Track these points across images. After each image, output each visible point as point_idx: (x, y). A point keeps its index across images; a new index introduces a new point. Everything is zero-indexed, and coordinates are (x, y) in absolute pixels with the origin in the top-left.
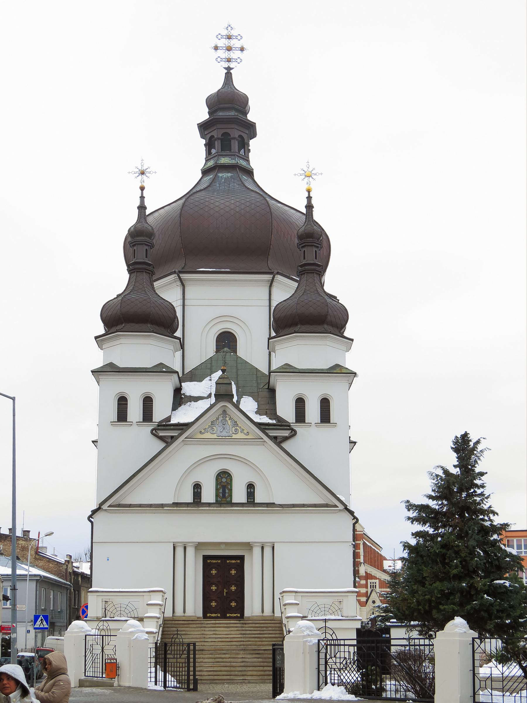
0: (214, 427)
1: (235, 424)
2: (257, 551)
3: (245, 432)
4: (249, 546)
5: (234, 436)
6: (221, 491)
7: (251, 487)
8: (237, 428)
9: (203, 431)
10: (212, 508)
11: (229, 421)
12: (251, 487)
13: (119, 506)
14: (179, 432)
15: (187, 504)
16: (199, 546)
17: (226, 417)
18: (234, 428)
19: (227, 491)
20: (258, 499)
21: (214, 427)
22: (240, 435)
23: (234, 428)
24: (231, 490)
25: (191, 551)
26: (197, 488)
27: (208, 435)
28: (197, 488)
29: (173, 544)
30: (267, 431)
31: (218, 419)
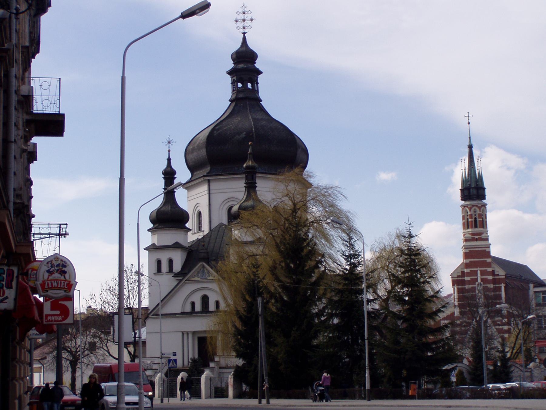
1: (209, 272)
5: (209, 278)
7: (217, 303)
11: (206, 271)
12: (217, 303)
22: (211, 278)
26: (193, 304)
27: (196, 278)
28: (193, 304)
31: (200, 270)
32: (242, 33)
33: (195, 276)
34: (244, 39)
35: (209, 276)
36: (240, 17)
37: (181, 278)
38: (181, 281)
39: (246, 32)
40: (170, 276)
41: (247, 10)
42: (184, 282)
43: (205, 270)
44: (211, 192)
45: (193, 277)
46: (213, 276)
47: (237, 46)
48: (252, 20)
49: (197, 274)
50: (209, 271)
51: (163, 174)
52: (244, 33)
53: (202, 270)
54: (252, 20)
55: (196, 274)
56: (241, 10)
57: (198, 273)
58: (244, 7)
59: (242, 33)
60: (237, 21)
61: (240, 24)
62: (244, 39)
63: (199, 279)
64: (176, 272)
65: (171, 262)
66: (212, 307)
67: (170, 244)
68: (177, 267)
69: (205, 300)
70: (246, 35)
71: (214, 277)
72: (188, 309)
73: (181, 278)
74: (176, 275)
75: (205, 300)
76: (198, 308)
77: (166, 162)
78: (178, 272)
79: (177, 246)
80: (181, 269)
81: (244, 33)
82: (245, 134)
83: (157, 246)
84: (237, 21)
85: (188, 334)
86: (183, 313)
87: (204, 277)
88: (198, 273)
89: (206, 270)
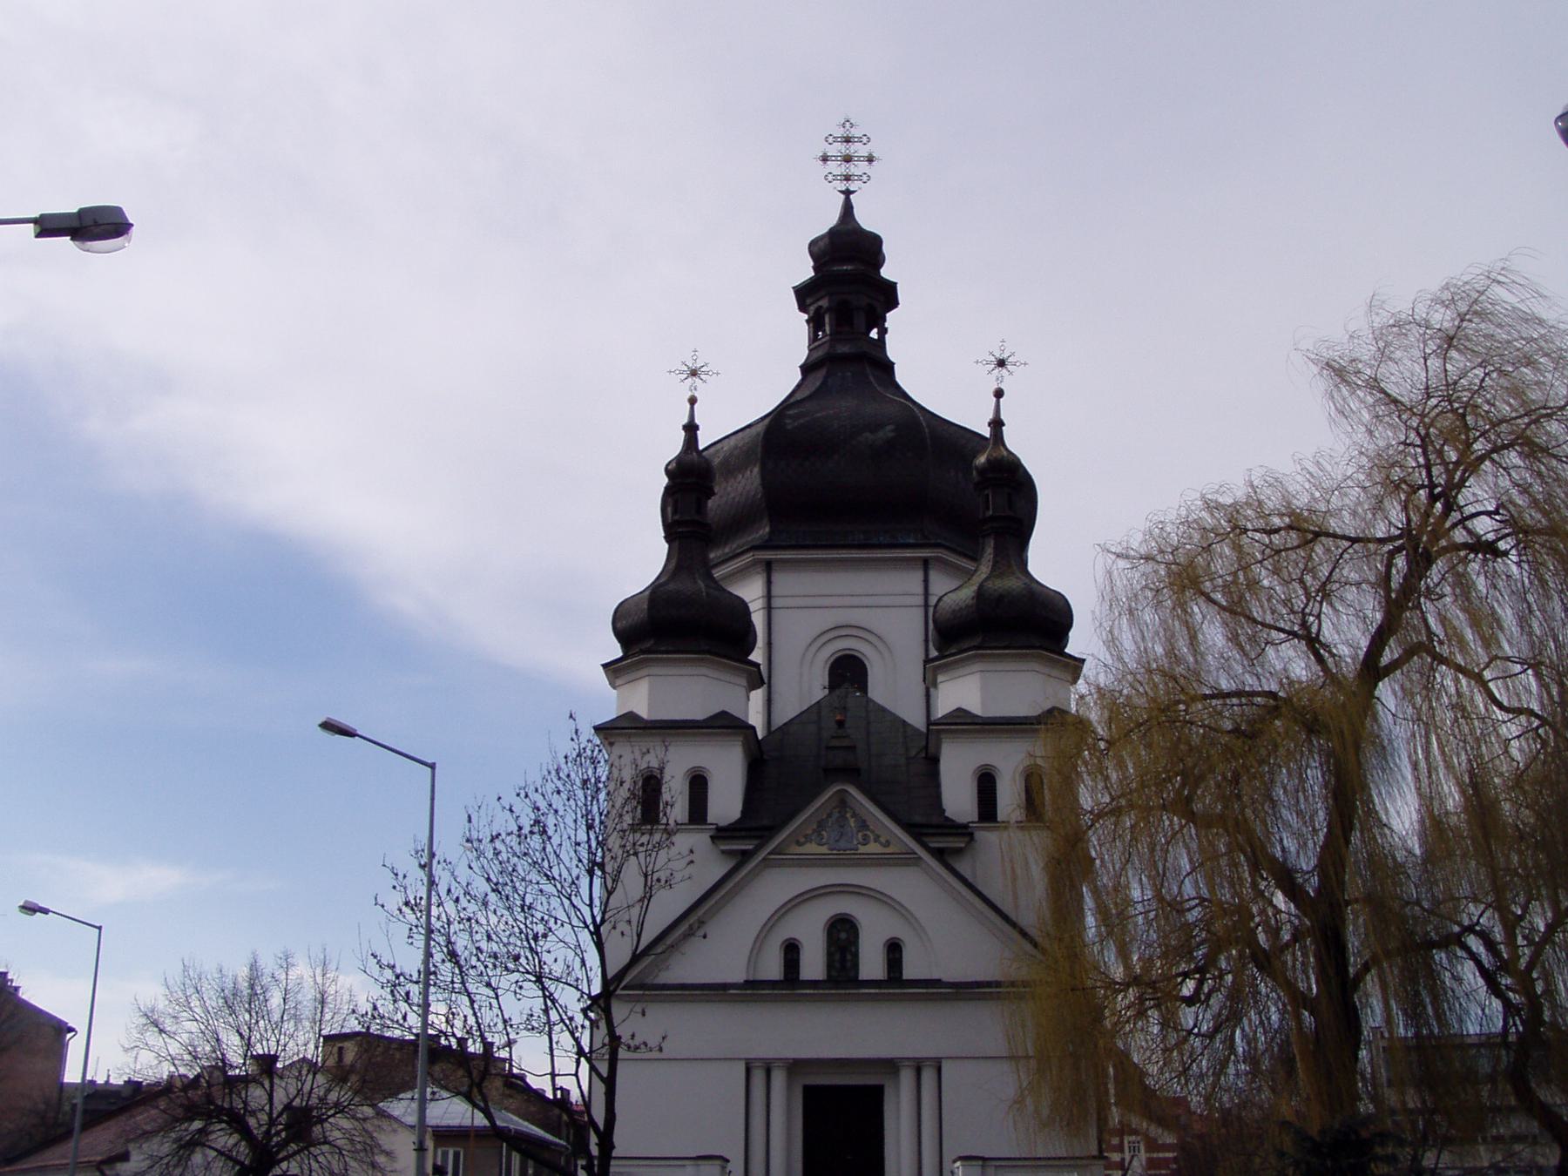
0: (824, 833)
1: (863, 825)
2: (906, 1077)
3: (883, 840)
4: (891, 1066)
5: (862, 849)
6: (837, 957)
7: (894, 949)
8: (868, 833)
9: (802, 840)
10: (821, 991)
11: (852, 822)
12: (894, 949)
13: (643, 986)
14: (756, 842)
15: (772, 984)
16: (795, 1067)
17: (846, 812)
18: (860, 834)
19: (849, 957)
20: (909, 972)
21: (824, 833)
22: (873, 848)
23: (860, 834)
24: (856, 955)
25: (778, 1079)
26: (792, 951)
27: (812, 848)
28: (792, 951)
29: (747, 1064)
30: (926, 839)
31: (829, 816)
32: (841, 192)
33: (806, 836)
34: (848, 209)
35: (865, 841)
36: (837, 149)
37: (747, 846)
38: (745, 856)
39: (852, 189)
40: (698, 840)
41: (855, 132)
42: (764, 859)
43: (848, 815)
44: (776, 602)
45: (799, 843)
46: (883, 840)
47: (829, 219)
48: (870, 159)
49: (814, 831)
50: (864, 821)
51: (667, 471)
52: (847, 193)
53: (836, 815)
54: (870, 159)
55: (809, 832)
56: (840, 132)
57: (821, 825)
58: (848, 124)
59: (841, 192)
60: (825, 159)
61: (836, 168)
62: (848, 209)
63: (824, 849)
64: (723, 823)
65: (698, 784)
66: (872, 965)
67: (699, 714)
68: (726, 802)
69: (842, 934)
70: (852, 196)
71: (887, 844)
72: (773, 968)
73: (747, 846)
74: (722, 834)
75: (842, 934)
76: (813, 965)
77: (680, 437)
78: (732, 824)
79: (725, 724)
80: (742, 812)
81: (847, 193)
82: (892, 431)
83: (647, 721)
84: (825, 159)
85: (768, 1072)
86: (750, 984)
87: (842, 844)
88: (821, 825)
89: (854, 815)
